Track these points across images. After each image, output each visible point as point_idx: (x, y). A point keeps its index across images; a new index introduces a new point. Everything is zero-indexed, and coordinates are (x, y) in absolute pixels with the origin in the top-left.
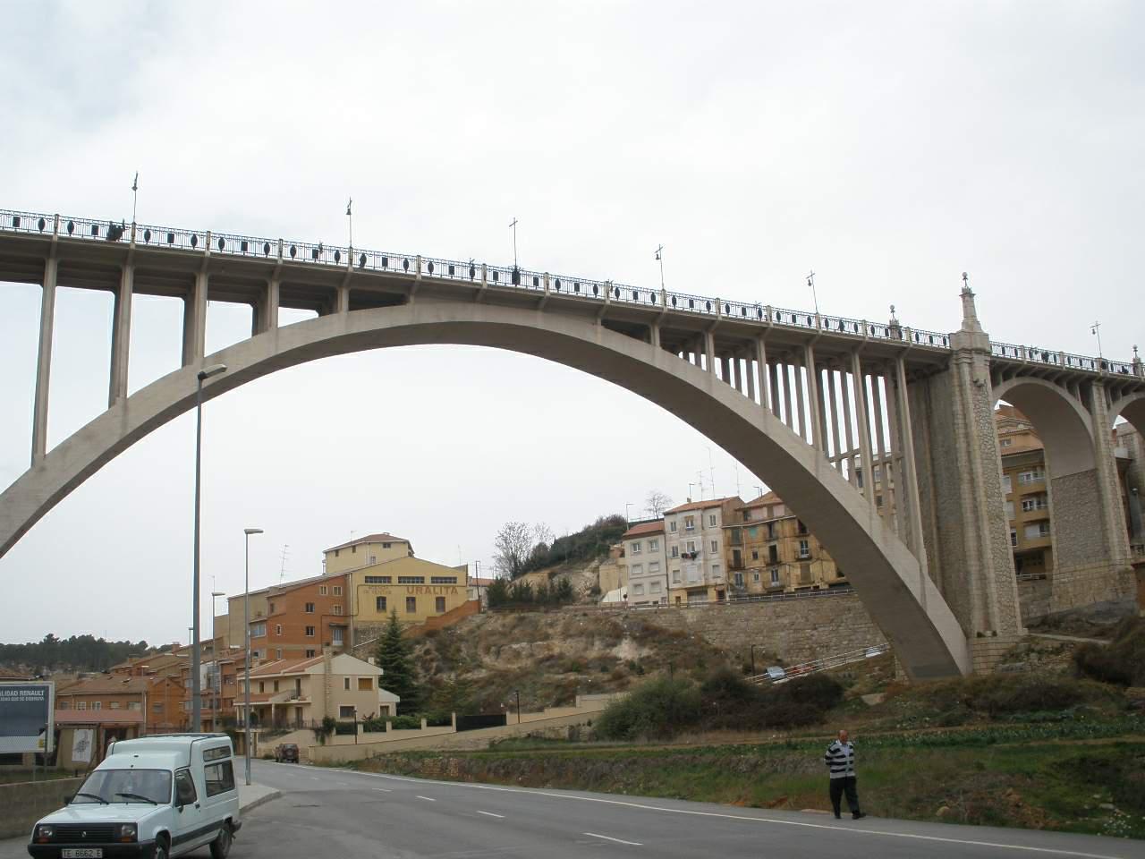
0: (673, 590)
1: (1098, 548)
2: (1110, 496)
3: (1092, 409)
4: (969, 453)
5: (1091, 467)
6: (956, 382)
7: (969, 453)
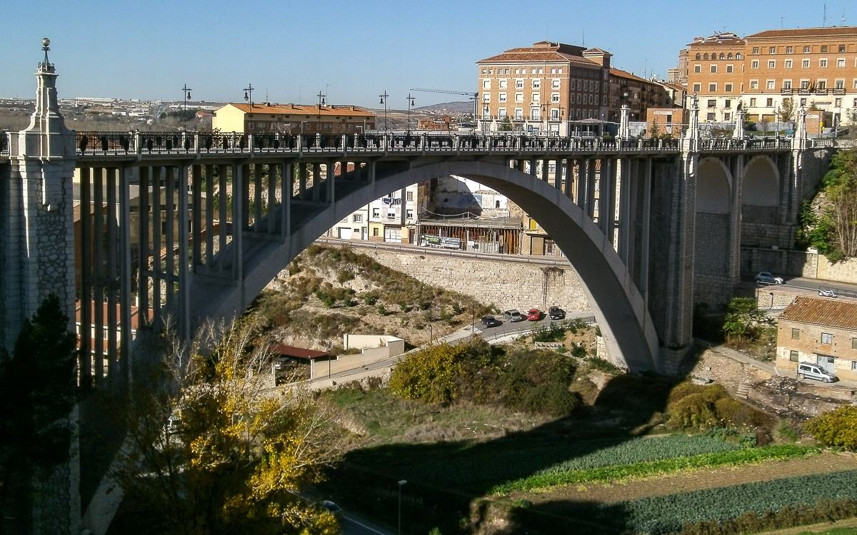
0: (372, 222)
1: (720, 267)
3: (734, 174)
4: (679, 224)
5: (726, 211)
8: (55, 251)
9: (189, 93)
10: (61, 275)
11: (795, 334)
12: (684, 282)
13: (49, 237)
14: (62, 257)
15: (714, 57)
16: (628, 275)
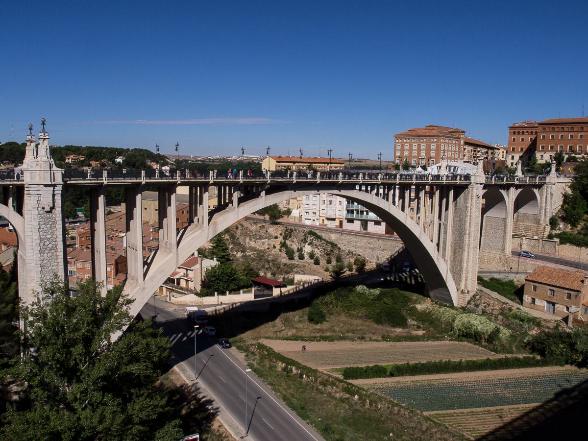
2: (509, 230)
5: (504, 217)
6: (470, 194)
7: (470, 223)
11: (535, 288)
12: (472, 256)
14: (55, 236)
15: (523, 132)
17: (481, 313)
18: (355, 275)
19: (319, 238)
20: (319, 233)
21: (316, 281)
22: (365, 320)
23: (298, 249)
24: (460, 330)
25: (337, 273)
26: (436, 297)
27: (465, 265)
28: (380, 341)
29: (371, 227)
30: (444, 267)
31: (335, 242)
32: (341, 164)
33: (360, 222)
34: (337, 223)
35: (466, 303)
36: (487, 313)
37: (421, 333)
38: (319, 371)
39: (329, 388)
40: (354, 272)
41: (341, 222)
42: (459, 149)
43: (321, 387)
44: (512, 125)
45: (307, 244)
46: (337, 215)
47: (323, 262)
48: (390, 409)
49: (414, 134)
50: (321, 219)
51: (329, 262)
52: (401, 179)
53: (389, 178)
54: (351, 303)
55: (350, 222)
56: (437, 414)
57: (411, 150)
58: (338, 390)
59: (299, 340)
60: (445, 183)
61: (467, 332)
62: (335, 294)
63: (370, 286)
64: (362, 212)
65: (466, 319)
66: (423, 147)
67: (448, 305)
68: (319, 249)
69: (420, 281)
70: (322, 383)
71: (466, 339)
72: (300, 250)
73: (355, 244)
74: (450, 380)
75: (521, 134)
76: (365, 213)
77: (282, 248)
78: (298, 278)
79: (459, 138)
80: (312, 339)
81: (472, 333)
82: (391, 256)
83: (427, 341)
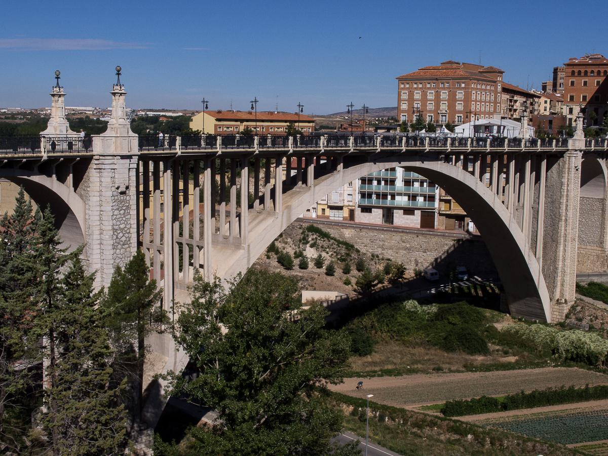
1: (596, 240)
4: (567, 206)
5: (602, 197)
6: (567, 166)
7: (567, 206)
8: (123, 222)
9: (207, 105)
10: (128, 239)
12: (570, 251)
13: (120, 211)
14: (128, 226)
15: (586, 72)
16: (527, 245)
17: (587, 329)
18: (388, 288)
19: (325, 236)
20: (325, 229)
21: (339, 298)
22: (428, 347)
23: (295, 253)
24: (567, 351)
25: (366, 286)
26: (519, 312)
27: (560, 264)
28: (463, 372)
29: (400, 219)
30: (535, 267)
31: (351, 242)
32: (309, 122)
33: (382, 210)
34: (346, 213)
35: (564, 318)
36: (596, 328)
37: (512, 359)
38: (409, 411)
39: (427, 430)
40: (386, 283)
41: (352, 212)
42: (496, 98)
43: (415, 430)
44: (567, 62)
45: (308, 245)
46: (345, 201)
47: (338, 272)
48: (521, 446)
49: (428, 75)
50: (320, 208)
51: (347, 271)
52: (430, 145)
53: (391, 144)
54: (401, 325)
55: (367, 212)
56: (585, 446)
57: (424, 99)
58: (441, 432)
59: (354, 377)
60: (539, 150)
61: (577, 354)
62: (376, 315)
63: (422, 302)
64: (385, 196)
65: (574, 336)
66: (444, 95)
67: (538, 321)
68: (327, 253)
69: (490, 291)
70: (416, 425)
71: (575, 363)
72: (299, 255)
73: (381, 243)
74: (579, 411)
75: (583, 74)
76: (389, 197)
77: (270, 254)
78: (307, 295)
79: (495, 82)
80: (371, 374)
81: (585, 353)
82: (436, 260)
83: (525, 368)
